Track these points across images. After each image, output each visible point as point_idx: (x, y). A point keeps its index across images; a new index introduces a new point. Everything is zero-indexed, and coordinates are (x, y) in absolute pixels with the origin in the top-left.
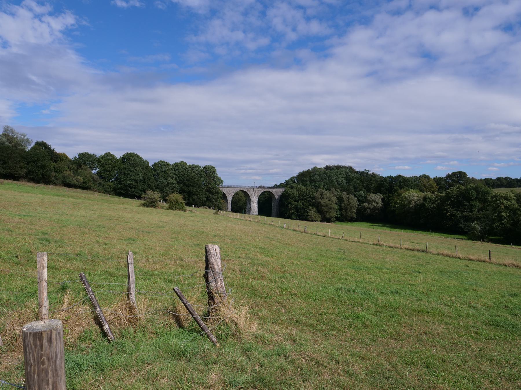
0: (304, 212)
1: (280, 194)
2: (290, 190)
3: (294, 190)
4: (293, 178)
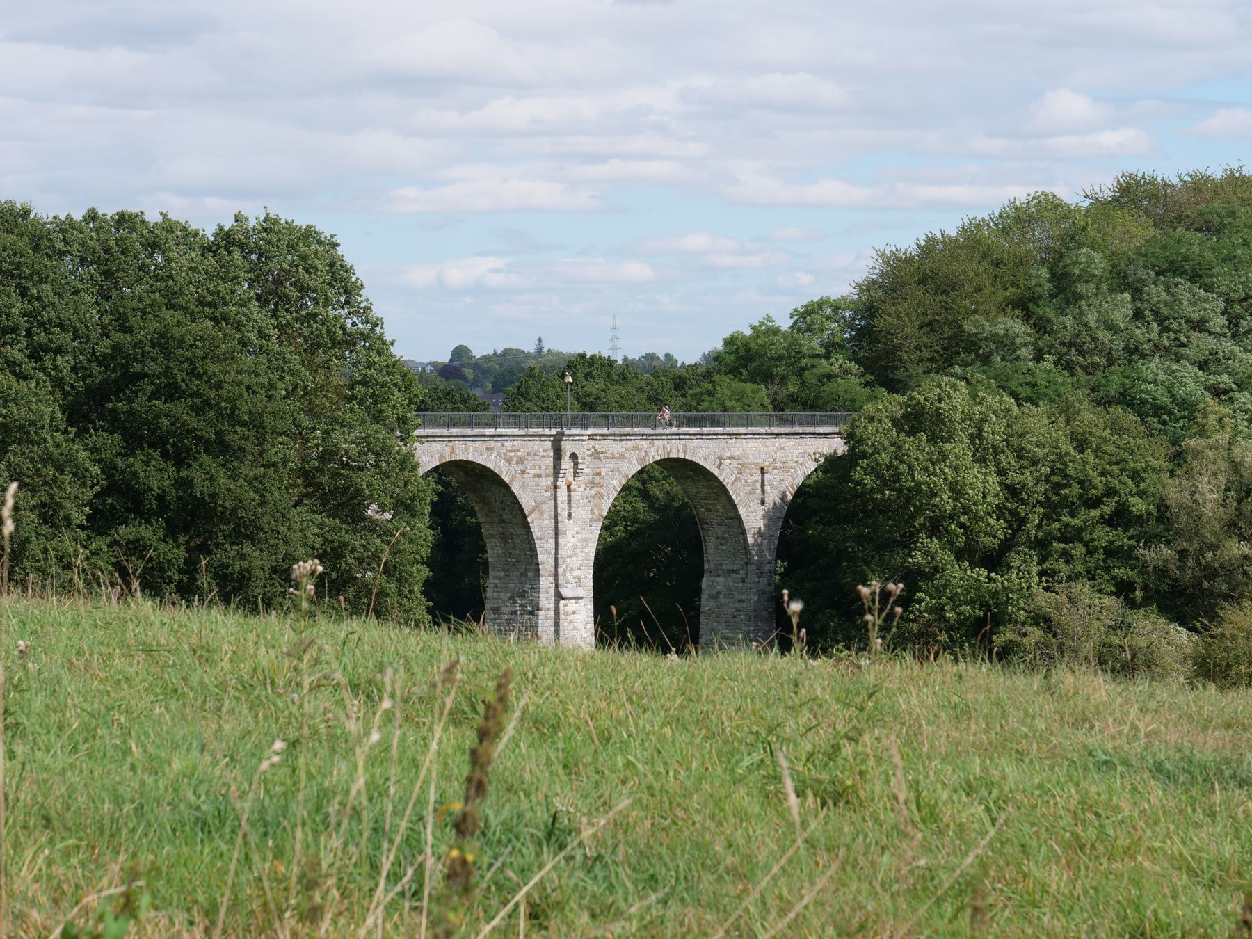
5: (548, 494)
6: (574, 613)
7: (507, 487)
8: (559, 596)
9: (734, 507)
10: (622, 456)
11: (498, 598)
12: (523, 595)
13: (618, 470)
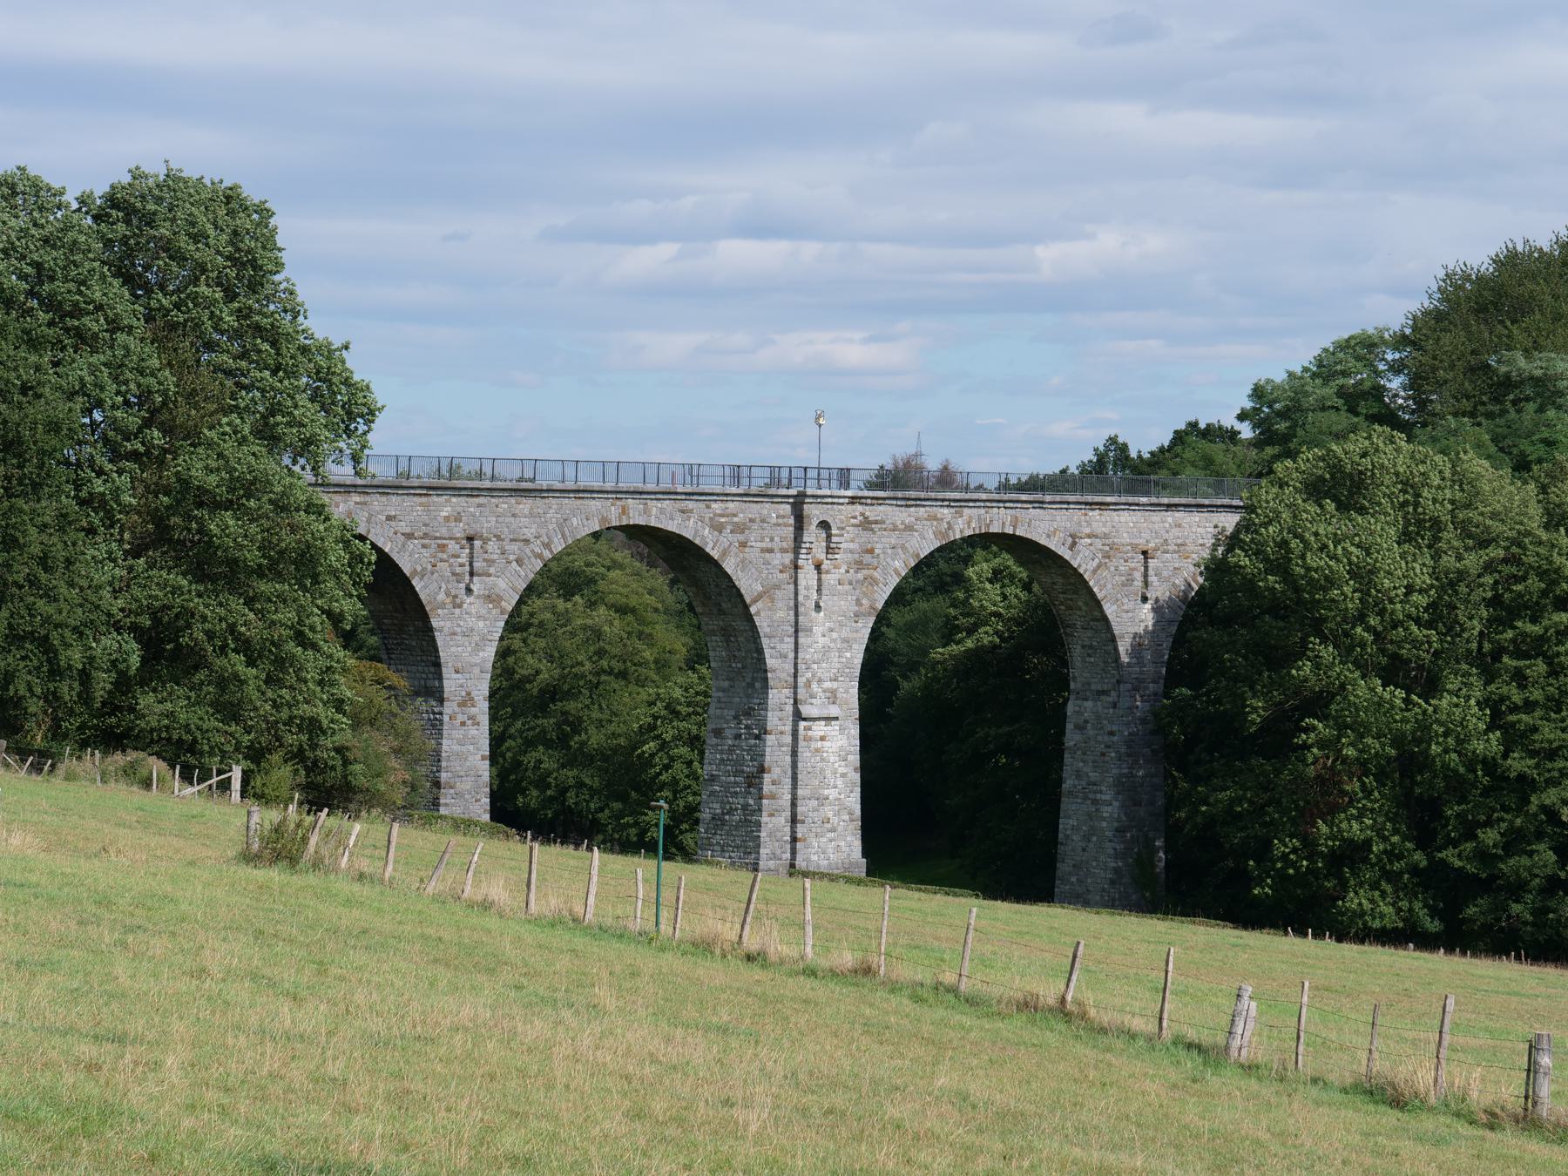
0: (1515, 842)
1: (1180, 572)
2: (1321, 521)
3: (1382, 529)
4: (1363, 347)
5: (786, 576)
6: (822, 739)
7: (716, 564)
8: (798, 716)
9: (1098, 603)
10: (909, 528)
11: (721, 717)
12: (748, 713)
13: (903, 547)
